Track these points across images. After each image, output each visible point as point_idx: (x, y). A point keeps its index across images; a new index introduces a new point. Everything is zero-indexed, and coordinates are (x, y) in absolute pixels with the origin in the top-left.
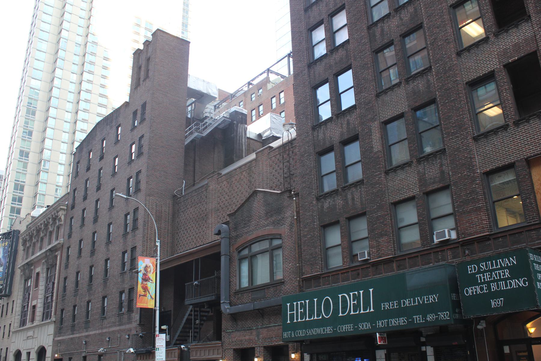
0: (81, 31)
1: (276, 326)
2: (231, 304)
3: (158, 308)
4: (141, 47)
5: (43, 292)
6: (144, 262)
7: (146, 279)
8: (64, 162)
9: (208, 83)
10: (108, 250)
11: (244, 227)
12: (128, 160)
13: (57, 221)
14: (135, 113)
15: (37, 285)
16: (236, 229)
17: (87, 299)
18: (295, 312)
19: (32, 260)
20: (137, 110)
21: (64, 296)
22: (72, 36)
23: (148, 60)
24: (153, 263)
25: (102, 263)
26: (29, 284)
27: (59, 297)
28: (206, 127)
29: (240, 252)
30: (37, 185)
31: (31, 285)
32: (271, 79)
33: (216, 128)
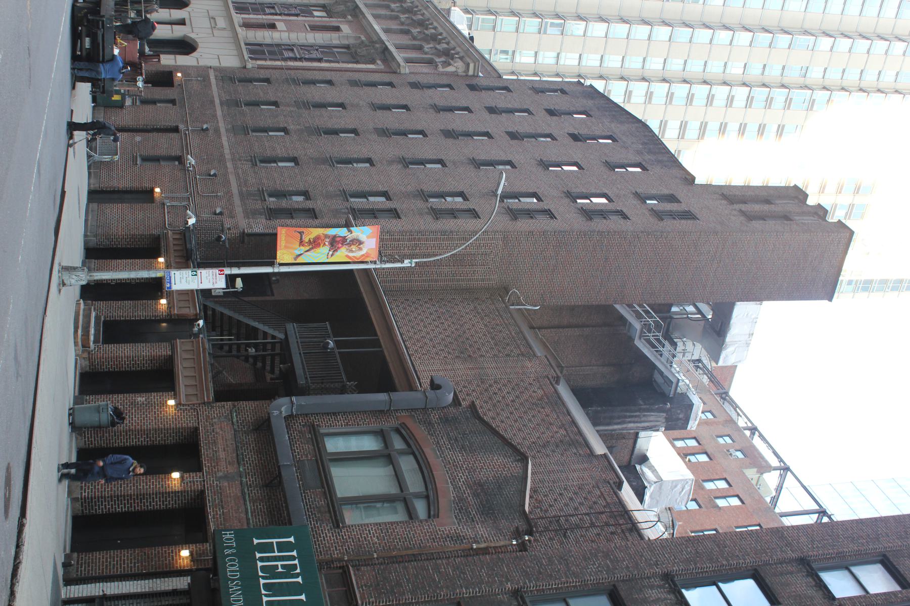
0: (834, 76)
2: (289, 418)
3: (276, 270)
4: (811, 201)
5: (302, 41)
6: (368, 237)
7: (335, 243)
8: (561, 62)
9: (748, 345)
10: (391, 162)
11: (450, 439)
12: (575, 191)
13: (443, 59)
14: (672, 198)
15: (315, 28)
16: (446, 420)
17: (291, 127)
18: (276, 554)
19: (365, 17)
20: (678, 201)
21: (296, 82)
22: (823, 58)
23: (786, 218)
24: (367, 255)
25: (365, 153)
26: (316, 13)
27: (292, 72)
28: (654, 346)
29: (398, 431)
30: (513, 13)
31: (314, 17)
32: (766, 476)
33: (654, 367)
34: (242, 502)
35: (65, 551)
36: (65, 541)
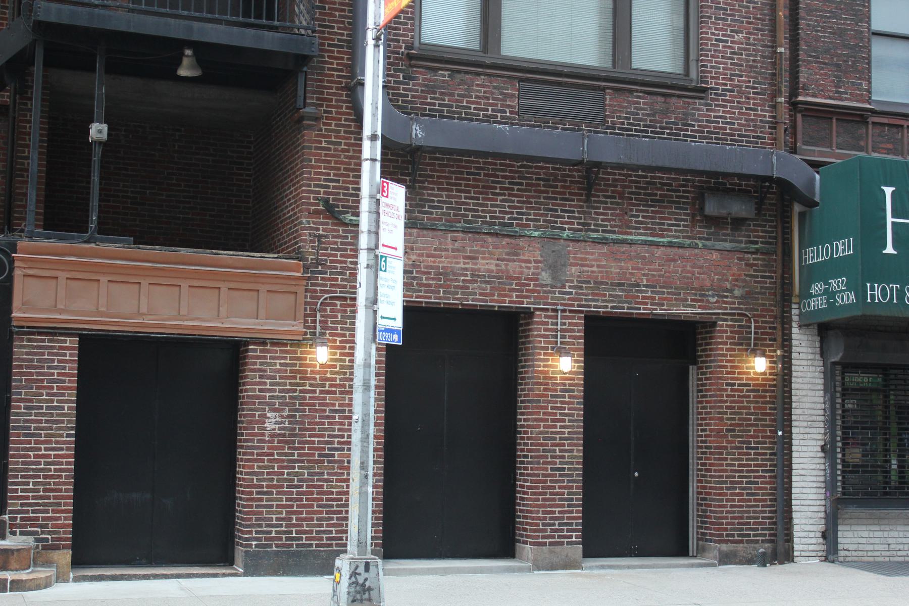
1: (657, 245)
34: (625, 248)
36: (692, 566)
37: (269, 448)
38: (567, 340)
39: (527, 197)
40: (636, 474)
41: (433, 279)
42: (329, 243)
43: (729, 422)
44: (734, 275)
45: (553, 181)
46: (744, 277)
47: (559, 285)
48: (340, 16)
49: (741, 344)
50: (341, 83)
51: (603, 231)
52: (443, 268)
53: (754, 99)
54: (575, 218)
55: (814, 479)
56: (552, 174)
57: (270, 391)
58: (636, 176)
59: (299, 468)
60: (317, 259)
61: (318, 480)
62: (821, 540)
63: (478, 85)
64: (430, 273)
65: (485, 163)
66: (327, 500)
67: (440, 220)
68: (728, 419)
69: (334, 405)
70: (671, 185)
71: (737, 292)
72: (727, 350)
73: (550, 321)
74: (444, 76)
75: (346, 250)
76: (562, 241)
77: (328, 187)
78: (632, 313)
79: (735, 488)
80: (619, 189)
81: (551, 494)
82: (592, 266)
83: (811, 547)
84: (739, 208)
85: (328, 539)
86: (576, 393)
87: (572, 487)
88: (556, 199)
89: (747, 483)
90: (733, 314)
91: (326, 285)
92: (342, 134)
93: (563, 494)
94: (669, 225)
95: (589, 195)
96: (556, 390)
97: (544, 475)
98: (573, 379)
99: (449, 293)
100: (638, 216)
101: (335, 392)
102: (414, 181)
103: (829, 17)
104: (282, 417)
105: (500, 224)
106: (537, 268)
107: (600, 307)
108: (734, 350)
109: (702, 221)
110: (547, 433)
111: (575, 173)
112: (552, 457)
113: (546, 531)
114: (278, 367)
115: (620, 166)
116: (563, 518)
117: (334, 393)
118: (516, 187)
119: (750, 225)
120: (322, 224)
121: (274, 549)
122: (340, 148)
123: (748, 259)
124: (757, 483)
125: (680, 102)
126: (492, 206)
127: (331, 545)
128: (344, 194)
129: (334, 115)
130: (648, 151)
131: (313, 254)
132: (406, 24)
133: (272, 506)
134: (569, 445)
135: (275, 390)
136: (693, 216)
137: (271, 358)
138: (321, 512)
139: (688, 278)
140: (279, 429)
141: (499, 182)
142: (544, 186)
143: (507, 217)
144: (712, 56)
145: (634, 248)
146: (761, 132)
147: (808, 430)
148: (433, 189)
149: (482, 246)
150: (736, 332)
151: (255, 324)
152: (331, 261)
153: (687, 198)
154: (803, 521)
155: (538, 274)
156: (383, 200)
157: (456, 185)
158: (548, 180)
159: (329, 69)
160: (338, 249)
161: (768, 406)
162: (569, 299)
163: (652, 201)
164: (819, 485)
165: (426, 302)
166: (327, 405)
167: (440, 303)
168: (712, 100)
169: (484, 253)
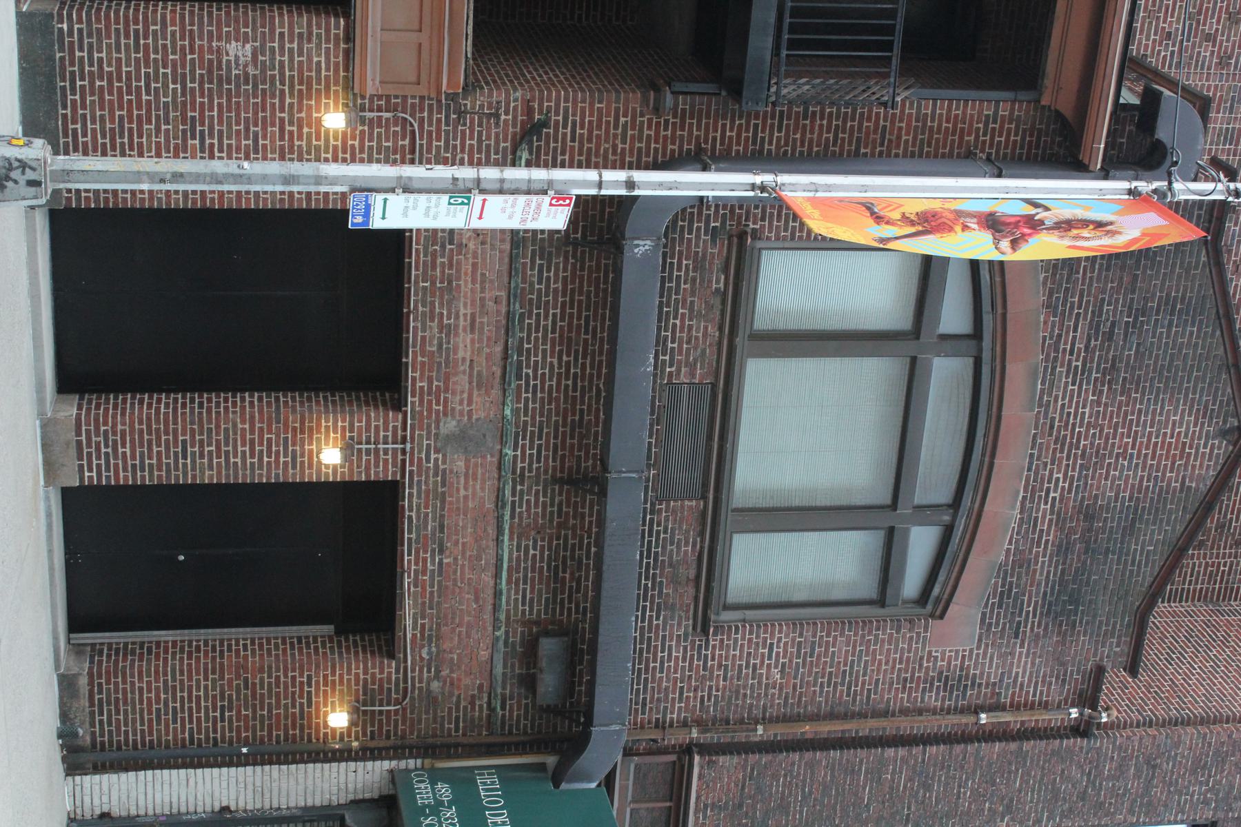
11: (1095, 327)
34: (492, 531)
35: (57, 667)
36: (55, 638)
37: (201, 47)
38: (364, 458)
39: (558, 399)
40: (182, 558)
41: (443, 272)
42: (489, 129)
43: (257, 681)
44: (459, 680)
45: (580, 433)
46: (456, 693)
47: (439, 445)
48: (795, 140)
49: (365, 694)
50: (706, 142)
51: (513, 502)
52: (459, 286)
53: (695, 697)
54: (530, 464)
55: (183, 799)
56: (589, 431)
57: (282, 48)
58: (589, 543)
59: (175, 90)
60: (466, 112)
61: (158, 117)
62: (98, 812)
63: (706, 328)
64: (451, 267)
65: (602, 339)
66: (131, 130)
67: (524, 281)
68: (262, 679)
69: (265, 138)
70: (578, 591)
71: (435, 685)
72: (357, 675)
73: (390, 434)
74: (718, 282)
75: (480, 152)
76: (499, 447)
77: (565, 127)
78: (403, 545)
79: (166, 693)
80: (571, 522)
81: (150, 442)
82: (466, 489)
83: (87, 800)
84: (549, 683)
85: (75, 130)
86: (291, 471)
87: (160, 470)
88: (556, 437)
89: (174, 708)
90: (405, 681)
91: (430, 124)
92: (637, 145)
93: (150, 458)
94: (524, 590)
95: (561, 482)
96: (294, 444)
97: (175, 431)
98: (310, 466)
99: (424, 294)
100: (535, 549)
101: (282, 138)
102: (575, 244)
103: (803, 791)
104: (246, 66)
105: (520, 363)
106: (461, 413)
107: (410, 501)
108: (357, 684)
109: (530, 634)
110: (235, 434)
111: (591, 462)
112: (201, 441)
113: (97, 435)
114: (315, 59)
115: (601, 523)
116: (116, 458)
117: (282, 138)
118: (570, 382)
119: (526, 698)
120: (515, 118)
121: (58, 55)
122: (618, 142)
123: (480, 699)
124: (175, 722)
125: (688, 600)
126: (544, 351)
127: (66, 135)
128: (555, 149)
129: (662, 133)
130: (623, 558)
131: (473, 107)
132: (786, 230)
133: (118, 51)
134: (219, 464)
135: (282, 55)
136: (537, 623)
137: (328, 49)
138: (112, 122)
139: (453, 618)
140: (229, 62)
141: (576, 359)
142: (573, 421)
143: (530, 371)
144: (750, 640)
145: (492, 544)
146: (651, 709)
147: (250, 787)
148: (565, 270)
149: (489, 339)
150: (381, 686)
151: (373, 27)
152: (463, 132)
153: (562, 614)
154: (124, 787)
155: (453, 417)
156: (547, 199)
157: (572, 301)
158: (580, 426)
159: (724, 126)
160: (480, 141)
161: (282, 733)
162: (420, 459)
163: (556, 567)
164: (175, 806)
165: (410, 263)
166: (264, 129)
167: (409, 282)
168: (693, 642)
169: (481, 340)
